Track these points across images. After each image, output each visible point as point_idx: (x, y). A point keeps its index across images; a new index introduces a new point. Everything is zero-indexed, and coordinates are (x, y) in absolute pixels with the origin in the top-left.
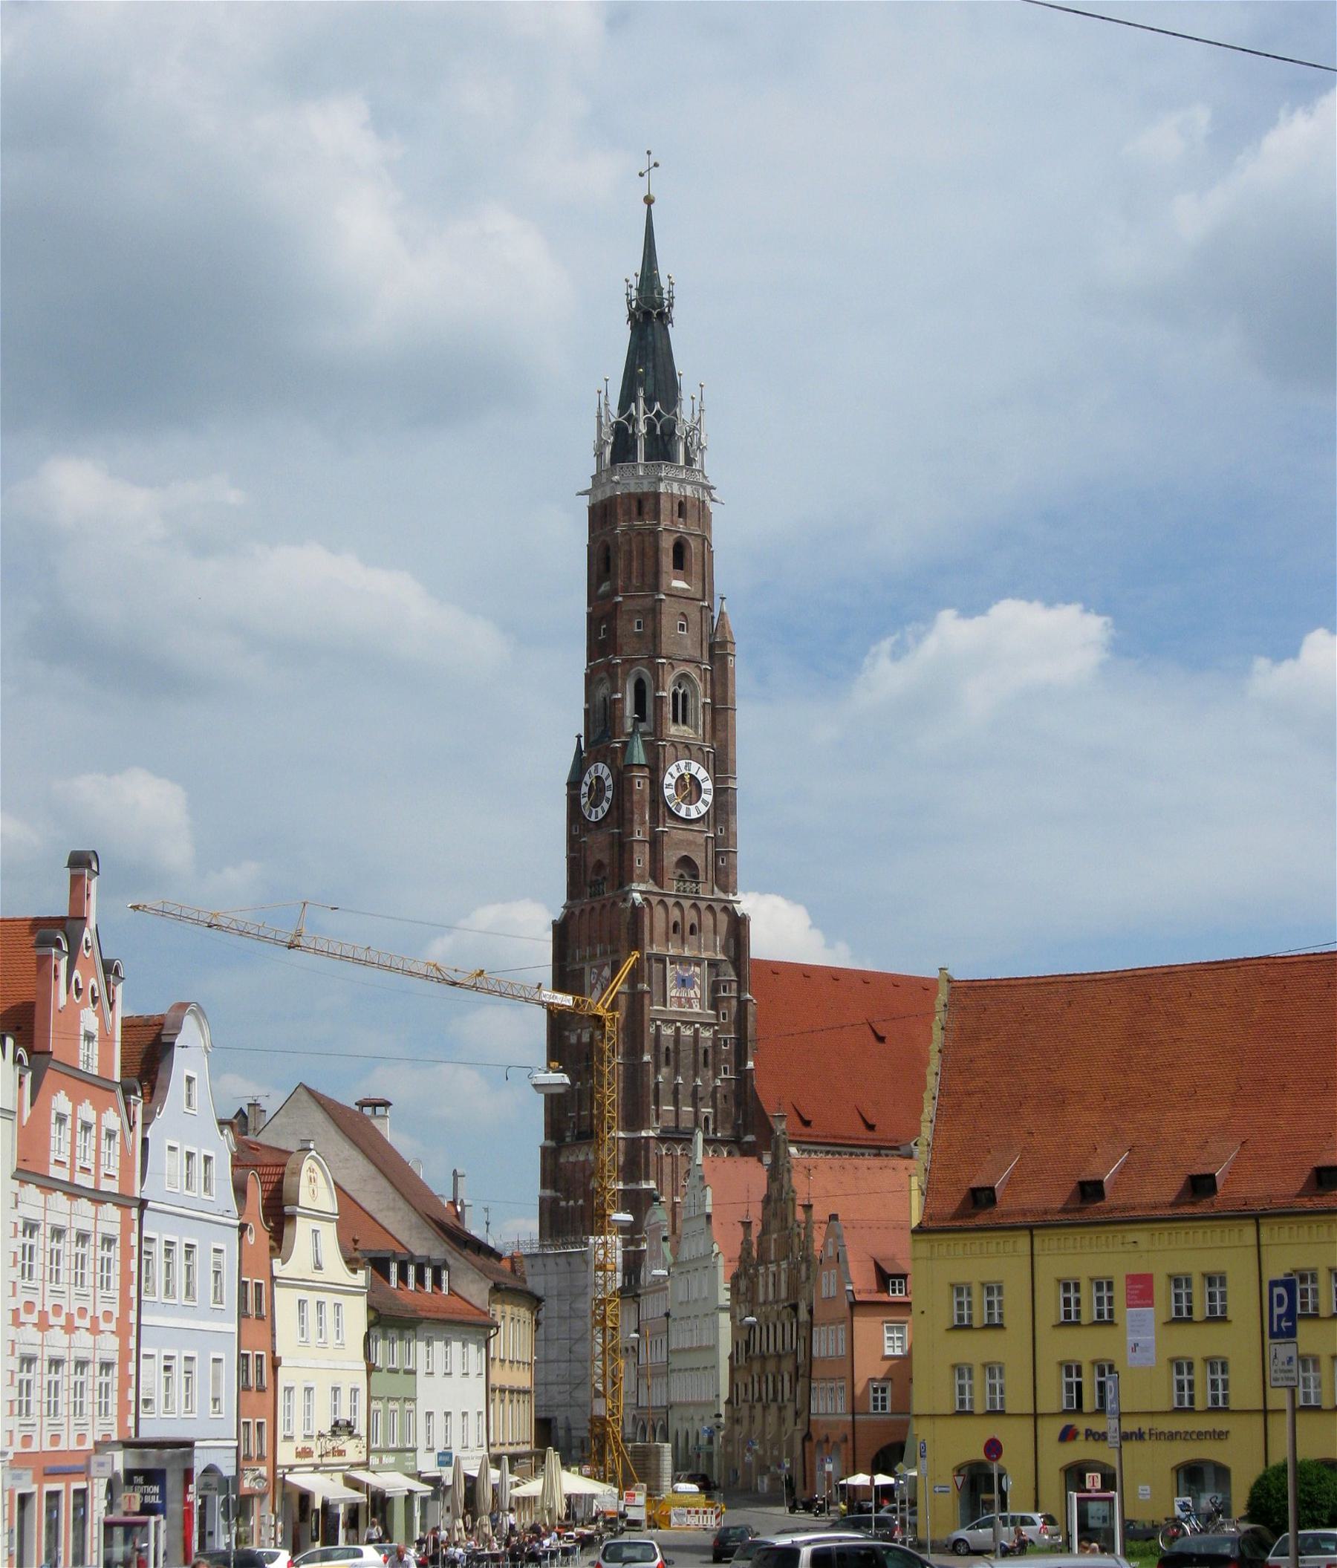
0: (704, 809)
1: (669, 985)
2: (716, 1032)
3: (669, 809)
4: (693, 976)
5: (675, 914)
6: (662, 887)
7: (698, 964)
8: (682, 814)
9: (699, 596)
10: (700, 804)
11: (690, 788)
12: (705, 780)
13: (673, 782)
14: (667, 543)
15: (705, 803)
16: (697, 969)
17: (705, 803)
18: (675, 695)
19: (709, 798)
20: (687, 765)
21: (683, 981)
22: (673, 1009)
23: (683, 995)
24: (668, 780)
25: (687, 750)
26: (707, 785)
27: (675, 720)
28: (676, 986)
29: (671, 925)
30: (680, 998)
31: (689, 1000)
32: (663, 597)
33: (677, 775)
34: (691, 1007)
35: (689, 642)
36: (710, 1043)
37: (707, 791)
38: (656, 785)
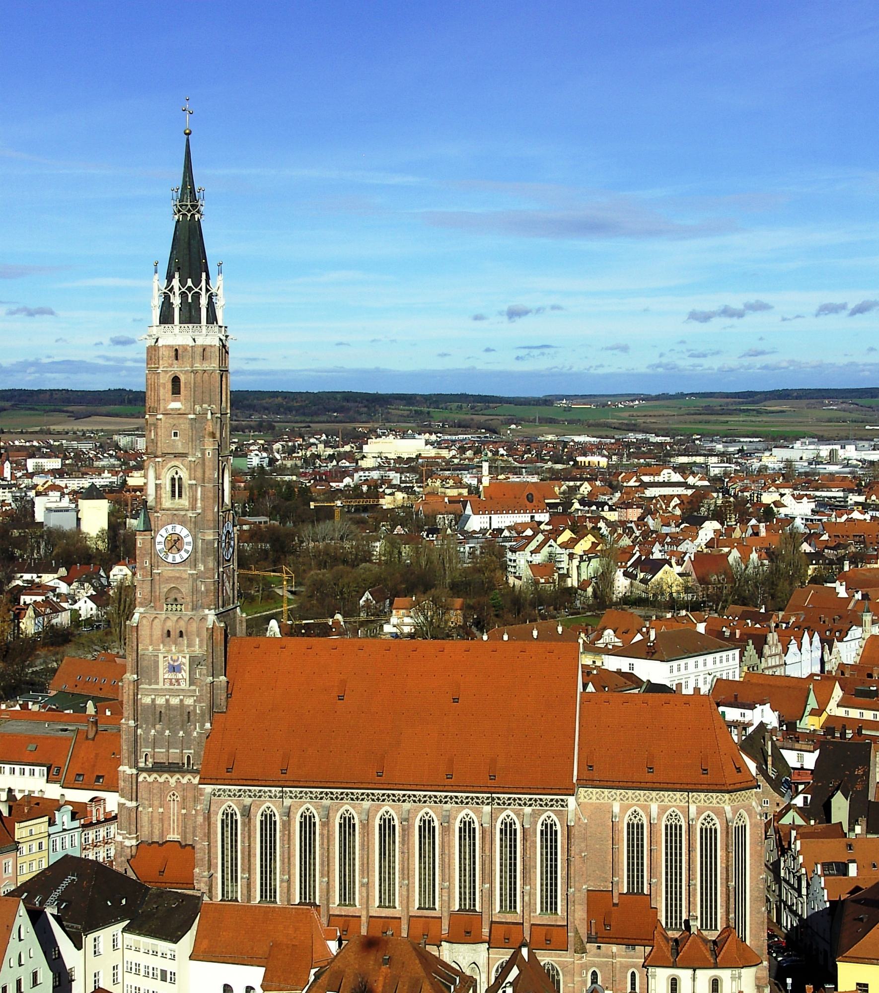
0: (185, 556)
1: (161, 671)
2: (195, 701)
4: (180, 665)
5: (169, 625)
7: (185, 657)
9: (187, 412)
10: (182, 552)
11: (175, 543)
12: (188, 535)
16: (184, 660)
18: (173, 479)
19: (190, 548)
24: (159, 539)
25: (176, 517)
26: (189, 539)
27: (173, 495)
28: (169, 671)
29: (166, 631)
31: (177, 680)
32: (159, 417)
33: (165, 535)
34: (179, 684)
35: (180, 444)
36: (192, 708)
37: (188, 544)
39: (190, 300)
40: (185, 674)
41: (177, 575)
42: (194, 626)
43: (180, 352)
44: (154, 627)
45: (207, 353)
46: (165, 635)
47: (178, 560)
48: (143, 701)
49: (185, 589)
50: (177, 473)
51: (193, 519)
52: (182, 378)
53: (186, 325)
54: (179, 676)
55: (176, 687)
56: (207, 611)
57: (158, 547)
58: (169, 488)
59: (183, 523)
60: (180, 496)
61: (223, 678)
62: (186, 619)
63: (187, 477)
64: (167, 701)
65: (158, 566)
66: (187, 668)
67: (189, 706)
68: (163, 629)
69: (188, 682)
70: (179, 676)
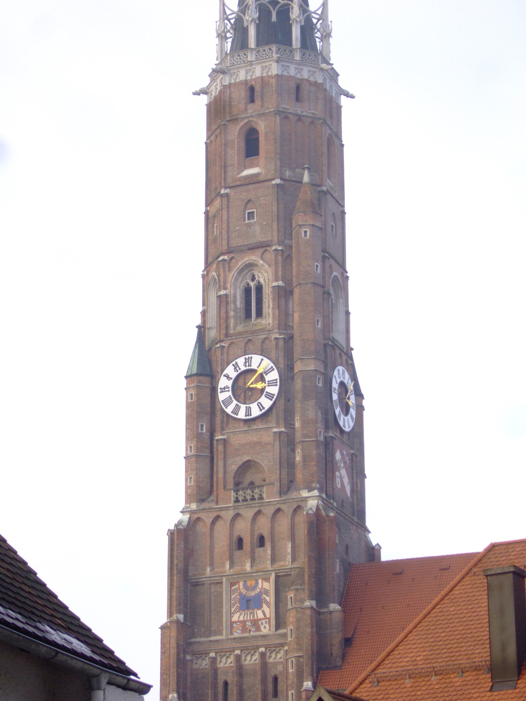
0: (267, 403)
3: (228, 415)
4: (260, 594)
6: (217, 503)
7: (267, 580)
8: (242, 415)
9: (269, 177)
13: (230, 383)
14: (235, 133)
15: (269, 396)
16: (266, 585)
17: (269, 396)
18: (247, 291)
20: (248, 361)
21: (248, 601)
22: (236, 635)
23: (249, 617)
24: (223, 382)
26: (274, 375)
28: (241, 609)
29: (235, 539)
30: (244, 622)
31: (256, 623)
34: (258, 629)
35: (257, 228)
36: (280, 668)
38: (214, 391)
39: (274, 18)
40: (267, 611)
41: (255, 439)
42: (283, 524)
43: (258, 89)
44: (216, 534)
45: (305, 93)
46: (235, 546)
47: (256, 412)
48: (195, 666)
49: (268, 461)
50: (253, 279)
51: (281, 343)
52: (261, 126)
53: (266, 48)
54: (260, 614)
55: (252, 633)
56: (305, 494)
57: (222, 396)
58: (240, 303)
59: (263, 353)
60: (259, 313)
61: (334, 607)
62: (269, 511)
63: (271, 278)
64: (238, 658)
65: (223, 429)
66: (271, 599)
67: (275, 664)
68: (231, 534)
69: (273, 622)
70: (260, 614)
